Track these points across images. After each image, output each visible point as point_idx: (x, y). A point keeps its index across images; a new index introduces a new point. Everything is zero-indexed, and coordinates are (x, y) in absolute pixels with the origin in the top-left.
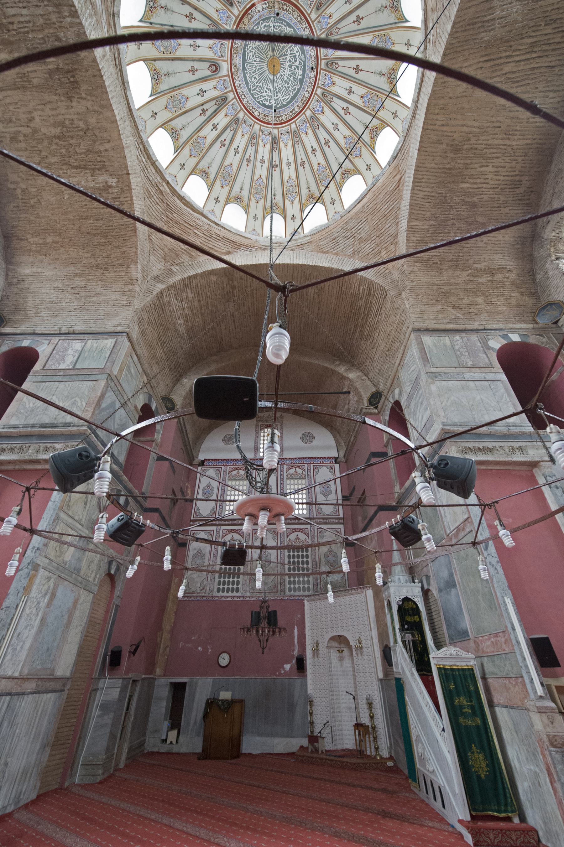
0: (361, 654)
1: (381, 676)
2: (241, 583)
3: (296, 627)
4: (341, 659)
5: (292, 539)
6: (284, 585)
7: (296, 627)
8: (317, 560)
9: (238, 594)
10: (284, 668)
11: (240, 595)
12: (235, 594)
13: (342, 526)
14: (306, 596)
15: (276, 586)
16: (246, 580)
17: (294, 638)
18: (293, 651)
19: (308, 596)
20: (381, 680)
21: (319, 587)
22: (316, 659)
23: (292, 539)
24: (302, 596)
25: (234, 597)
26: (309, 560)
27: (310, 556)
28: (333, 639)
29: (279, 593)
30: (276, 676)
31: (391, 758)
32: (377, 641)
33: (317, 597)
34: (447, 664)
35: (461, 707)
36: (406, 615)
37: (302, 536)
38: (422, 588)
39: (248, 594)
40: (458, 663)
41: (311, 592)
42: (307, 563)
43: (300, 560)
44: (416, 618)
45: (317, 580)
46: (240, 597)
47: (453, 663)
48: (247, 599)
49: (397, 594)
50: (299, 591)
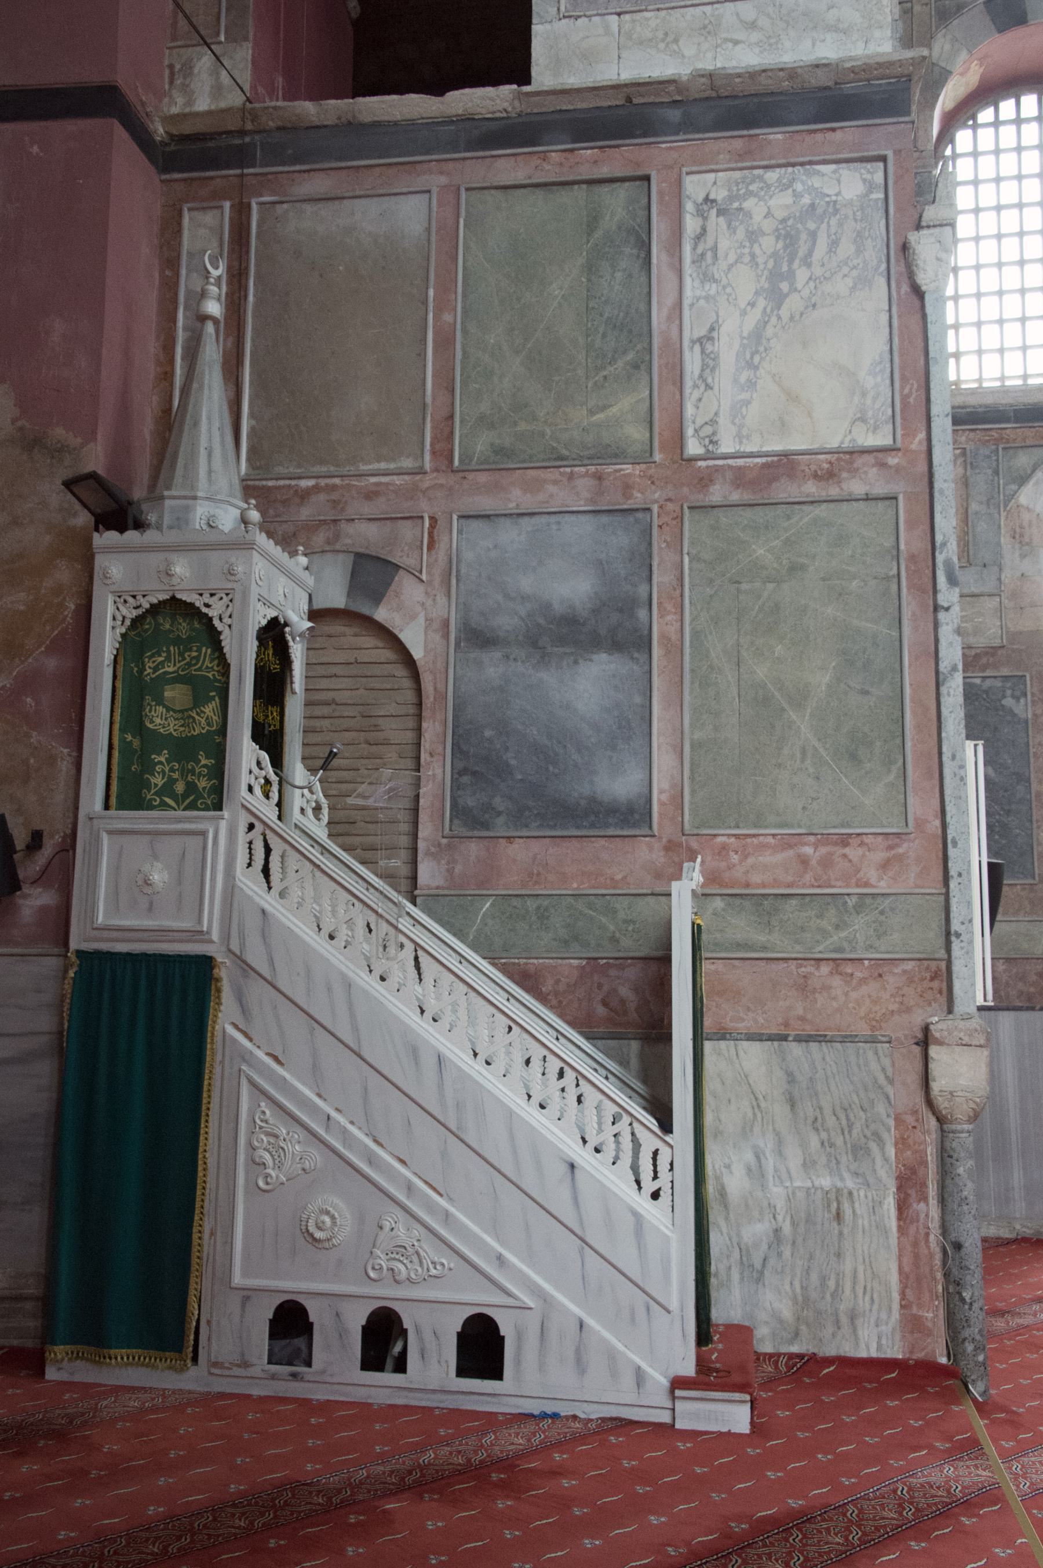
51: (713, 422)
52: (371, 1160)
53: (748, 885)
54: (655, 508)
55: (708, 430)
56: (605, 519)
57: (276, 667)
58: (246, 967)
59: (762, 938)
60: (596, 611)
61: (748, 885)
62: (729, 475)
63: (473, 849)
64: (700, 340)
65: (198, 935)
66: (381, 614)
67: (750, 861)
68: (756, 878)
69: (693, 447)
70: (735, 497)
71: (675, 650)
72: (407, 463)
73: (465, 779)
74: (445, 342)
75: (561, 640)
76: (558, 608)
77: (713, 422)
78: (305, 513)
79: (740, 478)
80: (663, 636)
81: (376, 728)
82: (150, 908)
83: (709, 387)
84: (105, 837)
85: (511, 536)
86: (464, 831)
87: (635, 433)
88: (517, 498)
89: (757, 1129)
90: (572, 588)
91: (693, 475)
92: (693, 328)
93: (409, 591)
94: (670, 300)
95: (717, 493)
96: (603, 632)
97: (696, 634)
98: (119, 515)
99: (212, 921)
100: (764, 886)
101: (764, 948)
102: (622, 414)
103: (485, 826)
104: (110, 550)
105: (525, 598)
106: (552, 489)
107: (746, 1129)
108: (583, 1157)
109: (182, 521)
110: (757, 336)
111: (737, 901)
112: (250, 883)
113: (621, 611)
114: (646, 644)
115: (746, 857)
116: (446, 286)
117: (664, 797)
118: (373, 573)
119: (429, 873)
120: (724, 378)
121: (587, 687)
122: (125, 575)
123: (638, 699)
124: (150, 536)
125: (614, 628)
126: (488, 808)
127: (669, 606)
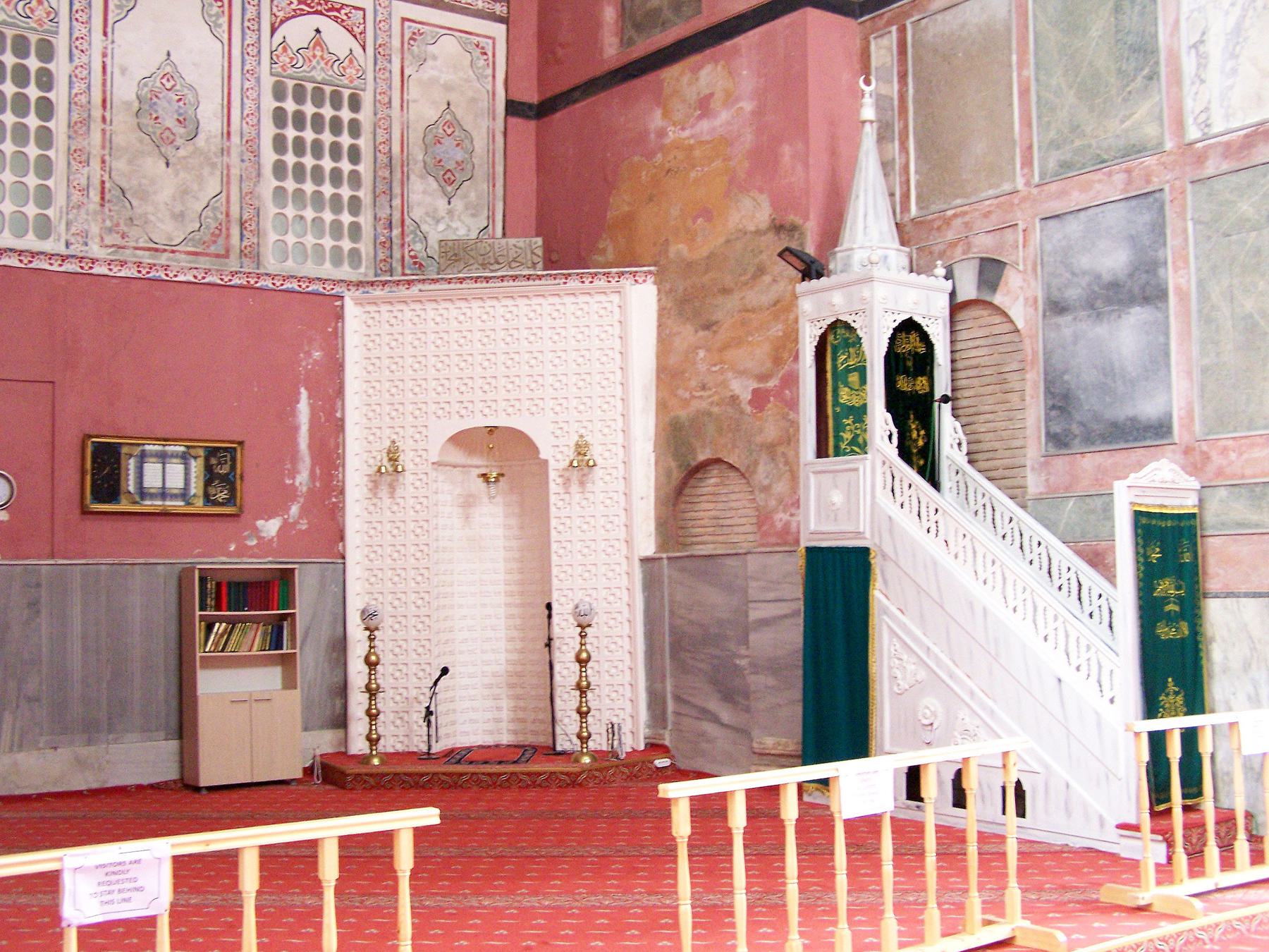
0: (582, 483)
1: (648, 547)
2: (60, 199)
3: (304, 393)
4: (468, 503)
5: (294, 44)
6: (258, 233)
7: (304, 393)
8: (396, 149)
9: (48, 246)
10: (256, 530)
11: (62, 250)
12: (30, 242)
13: (499, 30)
14: (349, 284)
15: (221, 231)
16: (85, 190)
17: (295, 429)
18: (293, 473)
19: (359, 284)
20: (645, 561)
21: (397, 254)
22: (387, 502)
23: (294, 44)
24: (336, 282)
25: (34, 254)
26: (363, 143)
27: (366, 127)
28: (461, 440)
29: (233, 264)
30: (230, 555)
31: (655, 747)
32: (650, 447)
33: (403, 291)
34: (1153, 503)
35: (1165, 600)
36: (898, 373)
37: (338, 40)
38: (953, 295)
39: (95, 250)
40: (1167, 502)
41: (364, 271)
42: (355, 154)
43: (327, 138)
44: (922, 382)
45: (390, 226)
46: (64, 258)
47: (1159, 501)
48: (97, 270)
49: (890, 306)
50: (320, 260)
51: (1207, 109)
52: (951, 676)
53: (1243, 477)
54: (1167, 188)
55: (1203, 117)
56: (1134, 203)
57: (922, 350)
58: (884, 556)
59: (1255, 518)
60: (1131, 275)
61: (1243, 477)
62: (1220, 150)
63: (1060, 464)
64: (1195, 46)
65: (859, 534)
66: (998, 299)
67: (1245, 456)
68: (1248, 472)
69: (1193, 133)
70: (1225, 167)
71: (1183, 296)
72: (1007, 187)
73: (1054, 413)
74: (1024, 92)
75: (1109, 301)
76: (1107, 277)
77: (1207, 109)
78: (950, 235)
79: (1228, 150)
80: (1178, 289)
81: (1005, 382)
82: (836, 520)
83: (1202, 81)
84: (812, 478)
85: (1074, 227)
86: (1052, 451)
87: (1151, 130)
88: (1077, 198)
89: (1254, 666)
90: (1113, 260)
91: (1192, 154)
92: (1187, 37)
93: (1012, 279)
94: (1171, 20)
95: (1210, 168)
96: (1136, 291)
97: (1200, 283)
98: (811, 270)
99: (864, 525)
100: (1254, 476)
101: (1257, 525)
102: (1141, 119)
103: (1066, 445)
104: (805, 294)
105: (1084, 273)
106: (1098, 186)
107: (1246, 667)
108: (1068, 674)
109: (846, 267)
110: (1238, 29)
111: (1236, 490)
112: (883, 498)
113: (1147, 272)
114: (1162, 295)
115: (1241, 454)
116: (1023, 53)
117: (1183, 413)
118: (991, 271)
119: (1034, 483)
120: (1213, 74)
121: (1126, 335)
122: (815, 307)
123: (1162, 339)
124: (833, 278)
125: (1141, 288)
126: (1067, 432)
127: (1180, 264)
